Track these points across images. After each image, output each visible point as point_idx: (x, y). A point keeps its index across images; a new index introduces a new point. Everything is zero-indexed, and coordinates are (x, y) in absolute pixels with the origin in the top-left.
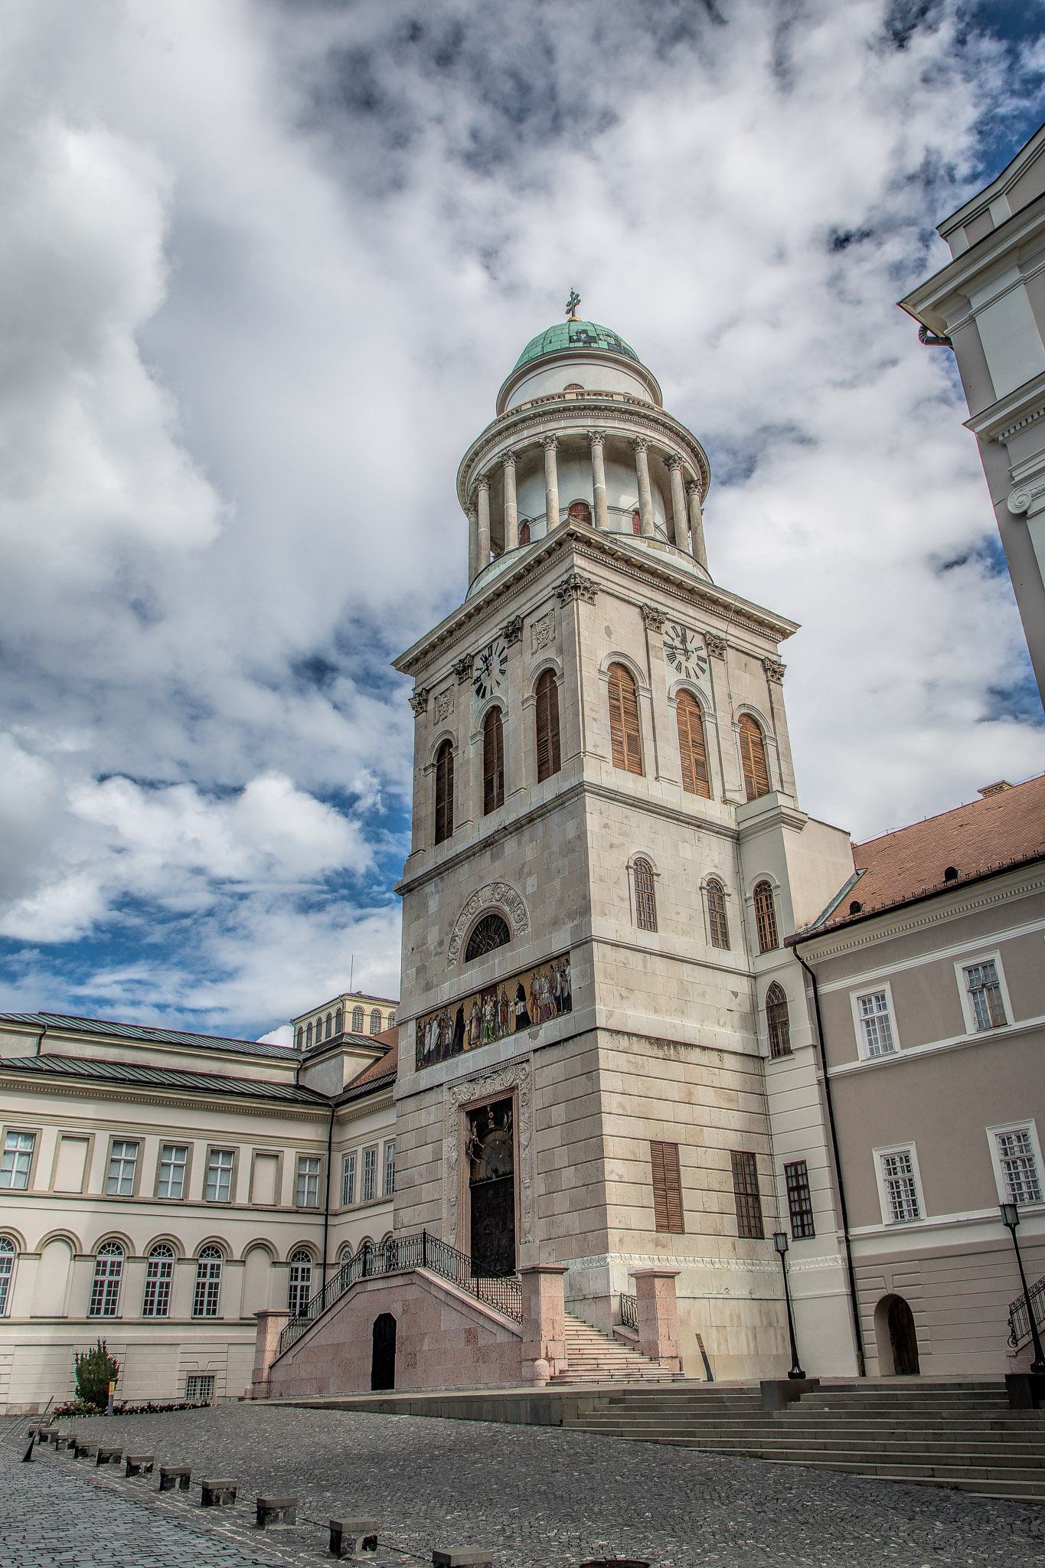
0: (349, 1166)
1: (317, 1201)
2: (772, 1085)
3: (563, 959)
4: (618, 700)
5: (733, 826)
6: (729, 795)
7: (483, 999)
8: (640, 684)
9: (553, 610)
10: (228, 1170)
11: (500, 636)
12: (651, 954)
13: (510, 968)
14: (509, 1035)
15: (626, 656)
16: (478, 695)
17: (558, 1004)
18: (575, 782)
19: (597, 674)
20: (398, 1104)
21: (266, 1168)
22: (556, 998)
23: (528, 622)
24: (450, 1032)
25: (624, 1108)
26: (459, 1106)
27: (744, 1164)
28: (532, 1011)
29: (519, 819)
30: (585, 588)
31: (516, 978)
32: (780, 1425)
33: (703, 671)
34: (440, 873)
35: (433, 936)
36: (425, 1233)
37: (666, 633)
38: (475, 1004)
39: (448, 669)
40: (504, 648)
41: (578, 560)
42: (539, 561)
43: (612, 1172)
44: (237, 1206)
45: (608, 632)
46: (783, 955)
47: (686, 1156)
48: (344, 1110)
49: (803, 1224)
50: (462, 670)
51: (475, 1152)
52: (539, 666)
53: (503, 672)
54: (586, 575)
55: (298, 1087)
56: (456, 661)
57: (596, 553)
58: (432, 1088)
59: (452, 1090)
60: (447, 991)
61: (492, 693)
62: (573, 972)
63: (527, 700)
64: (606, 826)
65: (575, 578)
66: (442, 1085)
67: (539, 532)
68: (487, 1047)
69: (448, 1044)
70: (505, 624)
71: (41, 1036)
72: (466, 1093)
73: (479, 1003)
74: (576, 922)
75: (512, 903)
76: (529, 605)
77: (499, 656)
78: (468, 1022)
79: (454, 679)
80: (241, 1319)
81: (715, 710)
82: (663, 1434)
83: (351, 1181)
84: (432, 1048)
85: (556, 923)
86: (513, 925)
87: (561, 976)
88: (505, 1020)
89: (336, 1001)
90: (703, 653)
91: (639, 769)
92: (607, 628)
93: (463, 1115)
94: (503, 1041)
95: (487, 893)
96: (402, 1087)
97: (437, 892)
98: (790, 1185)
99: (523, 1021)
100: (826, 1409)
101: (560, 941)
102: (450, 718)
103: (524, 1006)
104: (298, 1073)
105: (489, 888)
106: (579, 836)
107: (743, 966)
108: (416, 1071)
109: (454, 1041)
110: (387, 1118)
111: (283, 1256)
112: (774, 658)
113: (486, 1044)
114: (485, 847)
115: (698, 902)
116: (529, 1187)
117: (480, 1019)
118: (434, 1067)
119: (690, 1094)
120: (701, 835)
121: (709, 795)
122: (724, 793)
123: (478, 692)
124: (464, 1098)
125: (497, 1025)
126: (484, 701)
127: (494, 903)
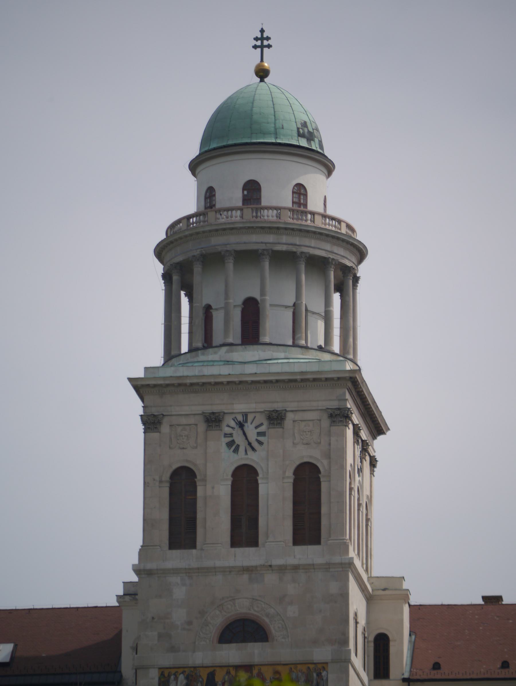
38: (228, 673)
78: (220, 683)
87: (317, 675)
127: (252, 612)
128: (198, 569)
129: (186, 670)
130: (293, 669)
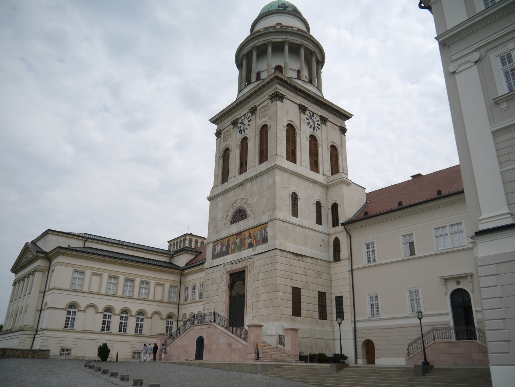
0: (187, 289)
1: (176, 300)
2: (333, 271)
3: (265, 225)
4: (289, 137)
5: (325, 183)
6: (325, 173)
7: (237, 237)
8: (297, 132)
9: (268, 104)
10: (147, 288)
11: (248, 112)
12: (296, 225)
13: (247, 227)
14: (245, 249)
15: (293, 122)
16: (239, 133)
17: (263, 240)
18: (273, 164)
19: (282, 127)
20: (206, 270)
21: (159, 289)
22: (262, 238)
23: (259, 108)
24: (224, 247)
25: (284, 276)
26: (227, 272)
27: (322, 296)
28: (254, 242)
29: (252, 176)
30: (280, 97)
31: (249, 231)
32: (336, 377)
33: (319, 129)
34: (223, 194)
35: (220, 215)
36: (215, 312)
37: (307, 115)
38: (234, 239)
39: (229, 123)
40: (250, 117)
41: (279, 87)
42: (264, 86)
43: (278, 296)
44: (149, 300)
45: (287, 113)
46: (340, 228)
47: (303, 292)
48: (186, 271)
49: (340, 314)
50: (235, 123)
51: (231, 286)
52: (262, 123)
53: (249, 125)
54: (281, 92)
55: (170, 263)
56: (232, 120)
57: (284, 84)
58: (218, 266)
59: (224, 267)
60: (224, 234)
61: (244, 132)
62: (268, 229)
63: (257, 135)
64: (283, 181)
65: (277, 93)
66: (221, 265)
67: (263, 76)
68: (237, 253)
69: (223, 252)
70: (250, 108)
71: (85, 241)
72: (229, 268)
73: (235, 238)
74: (271, 213)
75: (248, 205)
76: (259, 101)
77: (248, 119)
78: (231, 244)
79: (231, 126)
80: (150, 335)
81: (322, 143)
82: (297, 378)
83: (187, 295)
84: (218, 253)
85: (263, 213)
86: (248, 212)
87: (264, 231)
88: (244, 244)
89: (183, 236)
90: (319, 123)
91: (294, 161)
92: (287, 112)
93: (228, 275)
94: (243, 251)
95: (239, 201)
96: (206, 265)
97: (222, 200)
98: (337, 304)
99: (251, 245)
100: (352, 373)
101: (264, 219)
102: (229, 140)
103: (251, 240)
104: (170, 259)
105: (240, 200)
106: (273, 183)
107: (326, 231)
108: (212, 260)
109: (226, 251)
110: (202, 275)
111: (164, 317)
112: (343, 126)
113: (237, 252)
114: (239, 186)
115: (313, 209)
116: (250, 299)
117: (235, 243)
118: (219, 259)
119: (306, 272)
120: (315, 186)
121: (318, 172)
122: (323, 172)
123: (239, 132)
124: (229, 269)
125: (241, 246)
126: (241, 135)
127: (242, 205)
128: (225, 191)
129: (221, 241)
130: (256, 230)
